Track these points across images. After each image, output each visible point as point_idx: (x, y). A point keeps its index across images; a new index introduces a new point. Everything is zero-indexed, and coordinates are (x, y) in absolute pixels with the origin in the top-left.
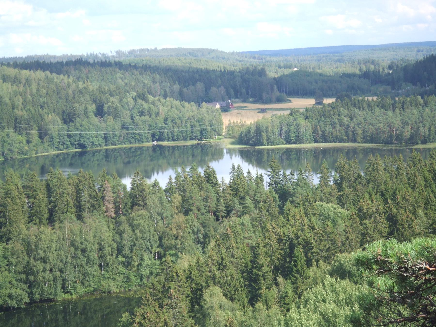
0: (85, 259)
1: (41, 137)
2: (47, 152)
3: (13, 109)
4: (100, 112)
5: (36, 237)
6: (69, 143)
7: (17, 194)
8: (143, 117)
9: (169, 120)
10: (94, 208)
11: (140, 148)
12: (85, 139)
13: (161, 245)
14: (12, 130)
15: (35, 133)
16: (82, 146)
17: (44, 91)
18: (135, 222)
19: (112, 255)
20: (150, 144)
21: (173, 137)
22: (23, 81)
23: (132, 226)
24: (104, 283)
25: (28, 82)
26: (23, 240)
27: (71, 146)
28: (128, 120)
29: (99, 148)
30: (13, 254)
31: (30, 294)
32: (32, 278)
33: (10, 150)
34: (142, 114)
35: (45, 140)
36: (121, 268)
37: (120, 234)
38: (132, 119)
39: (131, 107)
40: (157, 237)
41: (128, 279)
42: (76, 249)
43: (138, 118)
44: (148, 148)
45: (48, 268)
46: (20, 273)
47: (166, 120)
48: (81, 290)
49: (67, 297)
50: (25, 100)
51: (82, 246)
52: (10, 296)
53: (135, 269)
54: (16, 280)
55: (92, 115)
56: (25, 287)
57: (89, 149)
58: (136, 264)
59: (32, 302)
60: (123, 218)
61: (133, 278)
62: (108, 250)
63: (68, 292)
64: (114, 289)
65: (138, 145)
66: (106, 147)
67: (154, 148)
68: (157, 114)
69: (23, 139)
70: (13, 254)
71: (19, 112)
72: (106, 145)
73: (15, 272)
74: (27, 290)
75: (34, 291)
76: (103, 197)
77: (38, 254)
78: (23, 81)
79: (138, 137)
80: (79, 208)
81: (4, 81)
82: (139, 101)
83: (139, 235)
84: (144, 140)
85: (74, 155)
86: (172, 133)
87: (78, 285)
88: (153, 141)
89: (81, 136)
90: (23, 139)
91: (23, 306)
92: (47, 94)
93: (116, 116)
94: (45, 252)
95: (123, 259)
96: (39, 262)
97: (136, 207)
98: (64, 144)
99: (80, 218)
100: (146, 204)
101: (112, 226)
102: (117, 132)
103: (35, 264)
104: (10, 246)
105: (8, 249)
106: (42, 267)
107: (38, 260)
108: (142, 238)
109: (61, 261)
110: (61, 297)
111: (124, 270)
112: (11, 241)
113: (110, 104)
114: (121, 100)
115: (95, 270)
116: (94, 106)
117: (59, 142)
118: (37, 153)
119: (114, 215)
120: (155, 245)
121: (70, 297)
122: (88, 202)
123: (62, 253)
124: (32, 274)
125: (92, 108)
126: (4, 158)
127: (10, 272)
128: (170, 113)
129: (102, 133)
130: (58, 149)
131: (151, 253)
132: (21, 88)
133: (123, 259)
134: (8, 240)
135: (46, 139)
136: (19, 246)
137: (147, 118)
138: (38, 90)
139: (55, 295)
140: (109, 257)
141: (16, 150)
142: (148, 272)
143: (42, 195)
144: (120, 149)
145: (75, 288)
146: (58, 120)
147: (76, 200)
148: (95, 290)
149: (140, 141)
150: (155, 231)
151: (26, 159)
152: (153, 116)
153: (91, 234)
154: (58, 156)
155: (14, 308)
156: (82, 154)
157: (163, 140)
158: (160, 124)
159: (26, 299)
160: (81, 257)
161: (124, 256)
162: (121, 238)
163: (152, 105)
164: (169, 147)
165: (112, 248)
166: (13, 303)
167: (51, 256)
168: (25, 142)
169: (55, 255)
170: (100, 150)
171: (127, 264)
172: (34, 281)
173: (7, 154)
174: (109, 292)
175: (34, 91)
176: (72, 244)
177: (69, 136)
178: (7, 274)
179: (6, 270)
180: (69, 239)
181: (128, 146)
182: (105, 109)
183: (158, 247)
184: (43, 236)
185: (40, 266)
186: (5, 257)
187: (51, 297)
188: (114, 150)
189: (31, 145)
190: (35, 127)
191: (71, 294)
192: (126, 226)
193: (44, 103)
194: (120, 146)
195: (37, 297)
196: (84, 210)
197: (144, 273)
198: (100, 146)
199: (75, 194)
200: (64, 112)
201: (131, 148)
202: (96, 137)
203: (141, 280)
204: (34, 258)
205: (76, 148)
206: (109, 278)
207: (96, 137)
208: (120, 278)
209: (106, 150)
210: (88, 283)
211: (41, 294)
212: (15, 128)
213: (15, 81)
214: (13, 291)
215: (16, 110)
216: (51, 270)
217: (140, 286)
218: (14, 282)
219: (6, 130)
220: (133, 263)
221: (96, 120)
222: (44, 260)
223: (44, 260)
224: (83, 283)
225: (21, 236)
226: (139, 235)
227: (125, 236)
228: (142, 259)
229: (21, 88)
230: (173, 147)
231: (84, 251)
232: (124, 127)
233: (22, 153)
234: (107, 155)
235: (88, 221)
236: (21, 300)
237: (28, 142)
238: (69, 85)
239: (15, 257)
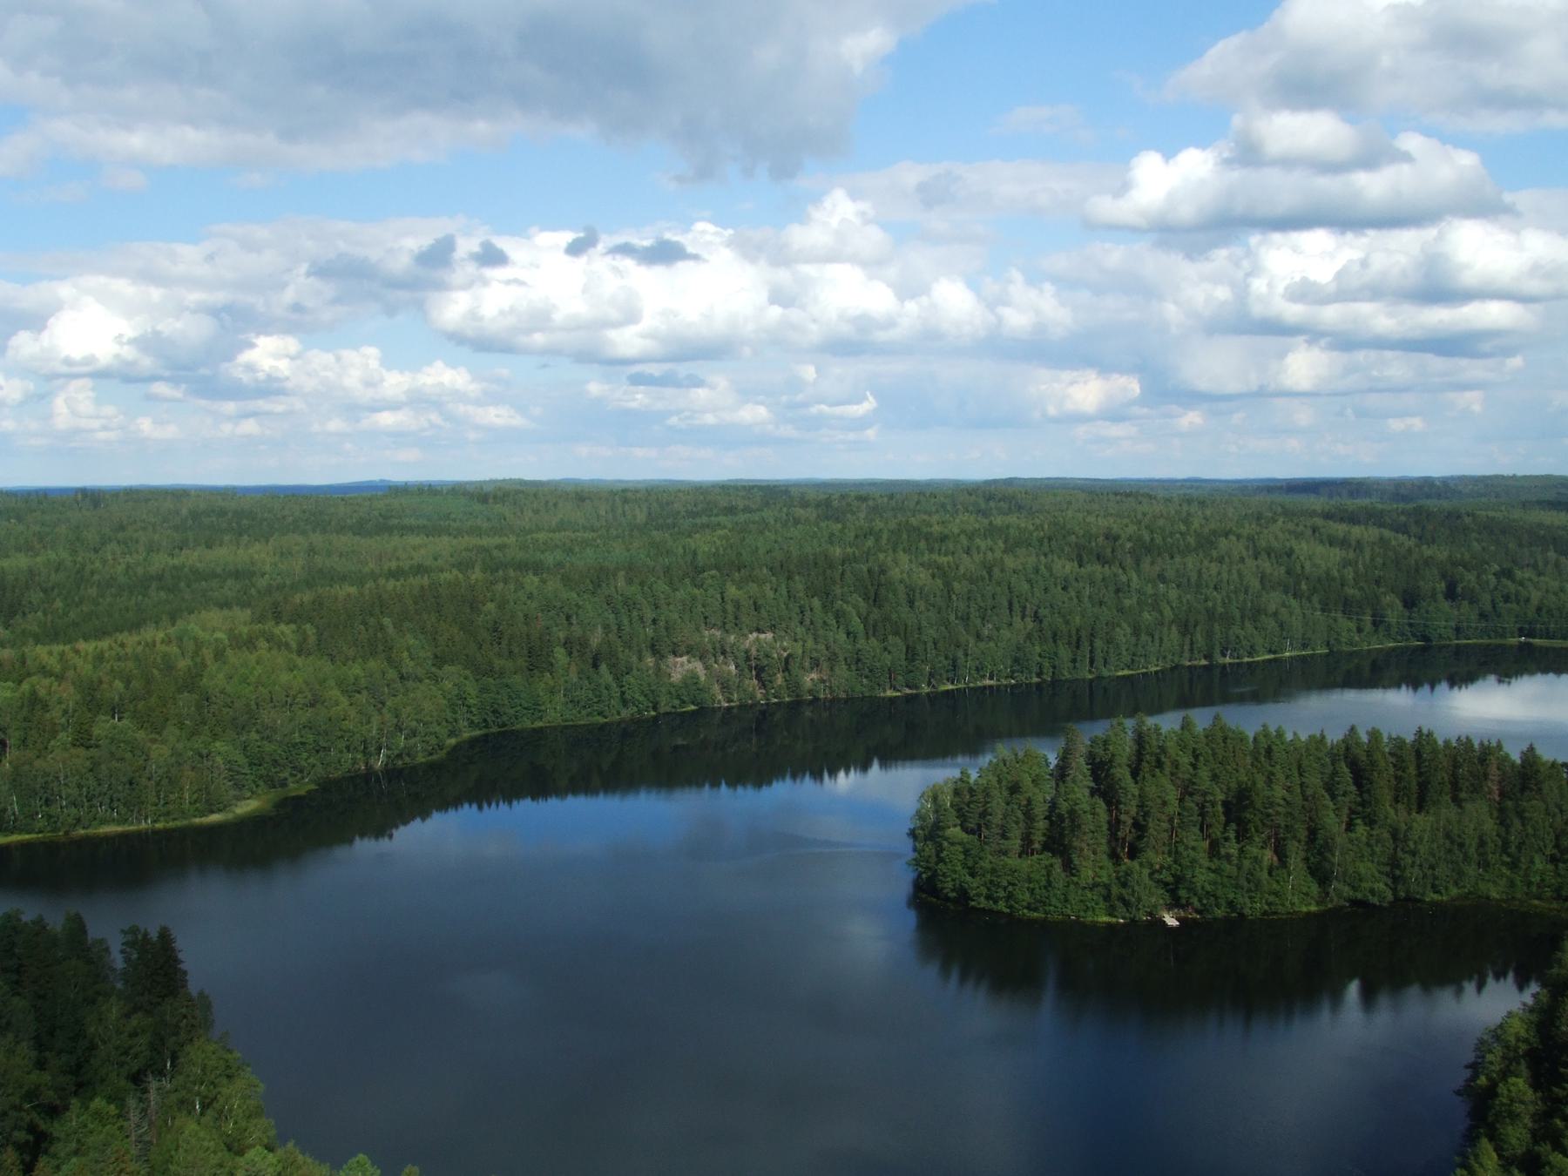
0: (1461, 856)
1: (1374, 623)
2: (1382, 644)
3: (1342, 585)
4: (1451, 594)
5: (1406, 825)
6: (1409, 634)
7: (1384, 765)
8: (1509, 605)
9: (1544, 610)
10: (1475, 790)
11: (1500, 646)
12: (1431, 631)
13: (1557, 846)
14: (1339, 615)
15: (1368, 618)
16: (1425, 638)
17: (1379, 560)
18: (1527, 815)
19: (1493, 853)
20: (1513, 641)
21: (1548, 633)
22: (1353, 543)
23: (1522, 818)
24: (1482, 886)
25: (1359, 546)
26: (1390, 826)
27: (1411, 637)
28: (1488, 607)
29: (1448, 642)
30: (1378, 841)
31: (1395, 890)
32: (1398, 872)
33: (1339, 642)
34: (1507, 599)
35: (1380, 629)
36: (1504, 870)
37: (1508, 827)
38: (1494, 607)
39: (1491, 587)
40: (1552, 836)
41: (1512, 884)
42: (1452, 842)
43: (1501, 605)
44: (1511, 647)
45: (1418, 862)
46: (1384, 864)
47: (1539, 610)
48: (1454, 891)
49: (1436, 897)
50: (1356, 572)
51: (1460, 841)
52: (1372, 891)
53: (1521, 873)
54: (1380, 872)
55: (1440, 597)
56: (1390, 882)
57: (1434, 643)
58: (1524, 867)
59: (1397, 899)
60: (1510, 804)
61: (1519, 883)
62: (1491, 845)
63: (1437, 892)
64: (1494, 895)
65: (1498, 641)
66: (1456, 642)
67: (1522, 646)
68: (1528, 600)
69: (1352, 625)
70: (1378, 841)
71: (1350, 591)
72: (1457, 639)
73: (1378, 862)
74: (1392, 885)
75: (1399, 887)
76: (1486, 776)
77: (1408, 846)
78: (1353, 543)
79: (1500, 630)
80: (1455, 786)
81: (1331, 545)
82: (1504, 581)
83: (1530, 831)
84: (1508, 635)
85: (1417, 648)
86: (1547, 629)
87: (1451, 886)
88: (1521, 636)
89: (1426, 626)
90: (1352, 625)
91: (1385, 905)
92: (1384, 564)
93: (1473, 601)
94: (1415, 843)
95: (1508, 860)
96: (1406, 855)
97: (1527, 793)
98: (1403, 634)
99: (1456, 800)
100: (1540, 789)
101: (1495, 814)
102: (1473, 625)
103: (1403, 856)
104: (1374, 833)
105: (1372, 835)
106: (1410, 861)
107: (1406, 852)
108: (1534, 835)
109: (1434, 856)
110: (1431, 896)
111: (1508, 873)
112: (1376, 827)
113: (1465, 584)
114: (1478, 577)
115: (1471, 871)
116: (1443, 585)
117: (1397, 632)
118: (1369, 644)
119: (1497, 798)
120: (1550, 846)
121: (1440, 898)
122: (1468, 780)
123: (1435, 845)
124: (1398, 866)
125: (1442, 586)
126: (1329, 649)
127: (1373, 862)
128: (1545, 601)
129: (1453, 624)
130: (1395, 640)
131: (1544, 854)
132: (1351, 555)
133: (1508, 860)
134: (1375, 822)
135: (1381, 629)
136: (1386, 835)
137: (1514, 606)
138: (1372, 560)
139: (1423, 894)
140: (1491, 856)
141: (1344, 640)
142: (1538, 878)
143: (1412, 770)
144: (1475, 644)
145: (1446, 888)
146: (1399, 604)
147: (1452, 775)
148: (1470, 893)
149: (1503, 636)
150: (1551, 827)
151: (1355, 652)
152: (1522, 603)
153: (1472, 826)
154: (1394, 649)
155: (1374, 906)
156: (1424, 649)
157: (1534, 637)
158: (1531, 613)
159: (1389, 896)
160: (1456, 852)
161: (1509, 855)
162: (1508, 832)
163: (1520, 588)
164: (1541, 647)
165: (1496, 845)
166: (1375, 900)
167: (1423, 849)
168: (1355, 629)
169: (1427, 847)
170: (1449, 645)
171: (1514, 865)
172: (1399, 877)
173: (1333, 645)
174: (1488, 898)
175: (1368, 561)
176: (1448, 836)
177: (1411, 625)
178: (1370, 864)
179: (1368, 860)
180: (1444, 830)
181: (1485, 641)
182: (1459, 590)
183: (1554, 847)
184: (1415, 824)
185: (1409, 860)
186: (1368, 844)
187: (1418, 897)
188: (1467, 646)
189: (1362, 635)
190: (1369, 611)
191: (1441, 894)
192: (1517, 823)
193: (1380, 577)
194: (1475, 641)
195: (1402, 894)
196: (1461, 790)
197: (1533, 880)
198: (1450, 640)
199: (1451, 768)
200: (1405, 591)
201: (1489, 645)
202: (1445, 628)
203: (1529, 887)
204: (1402, 850)
205: (1418, 641)
206: (1489, 881)
207: (1445, 628)
208: (1503, 882)
209: (1457, 644)
210: (1462, 884)
211: (1407, 892)
212: (1344, 612)
213: (1344, 543)
214: (1376, 886)
215: (1346, 588)
216: (1421, 866)
217: (1527, 894)
218: (1377, 874)
219: (1333, 614)
220: (1520, 865)
221: (1445, 605)
222: (1414, 853)
223: (1414, 853)
224: (1456, 884)
225: (1388, 821)
226: (1530, 831)
227: (1512, 830)
228: (1532, 862)
229: (1351, 555)
230: (1547, 649)
231: (1461, 845)
232: (1483, 616)
233: (1351, 644)
234: (1459, 651)
235: (1468, 806)
236: (1384, 898)
237: (1360, 630)
238: (1410, 551)
239: (1379, 845)
